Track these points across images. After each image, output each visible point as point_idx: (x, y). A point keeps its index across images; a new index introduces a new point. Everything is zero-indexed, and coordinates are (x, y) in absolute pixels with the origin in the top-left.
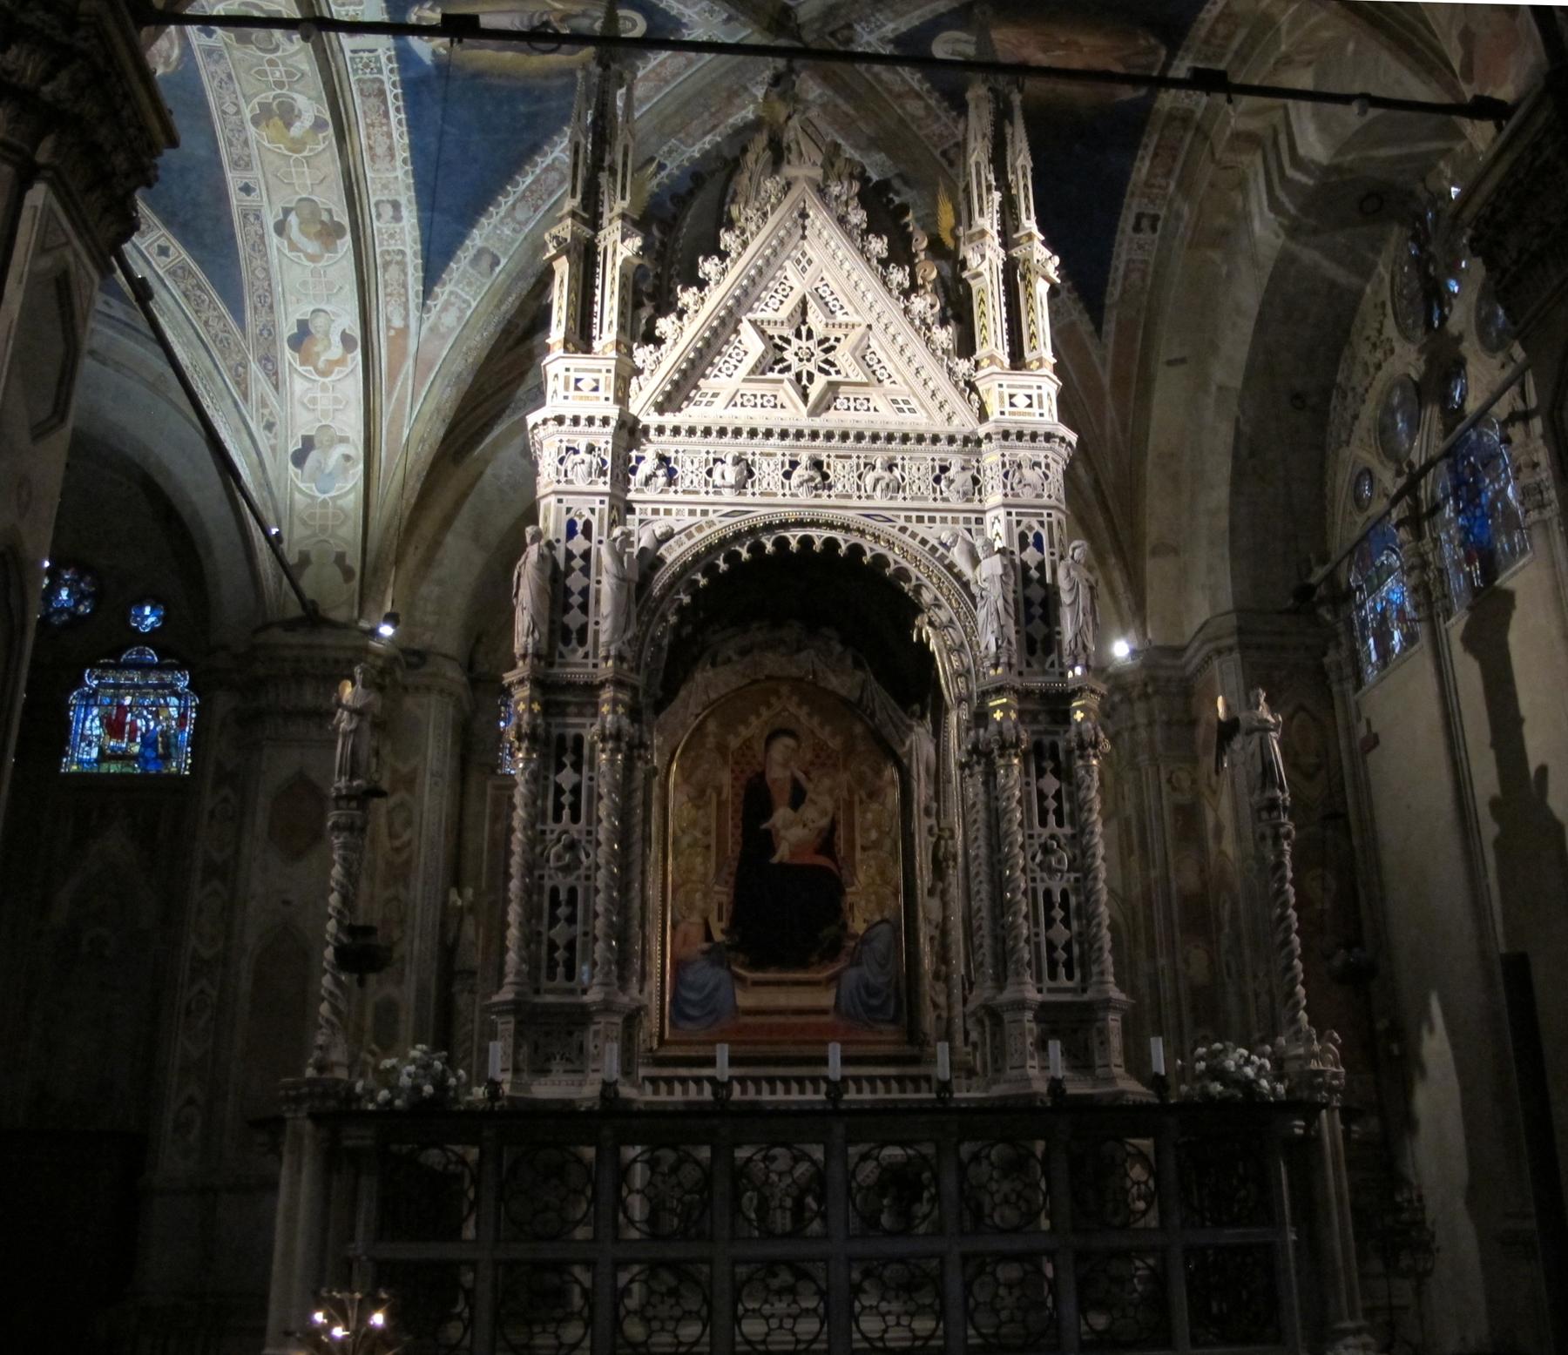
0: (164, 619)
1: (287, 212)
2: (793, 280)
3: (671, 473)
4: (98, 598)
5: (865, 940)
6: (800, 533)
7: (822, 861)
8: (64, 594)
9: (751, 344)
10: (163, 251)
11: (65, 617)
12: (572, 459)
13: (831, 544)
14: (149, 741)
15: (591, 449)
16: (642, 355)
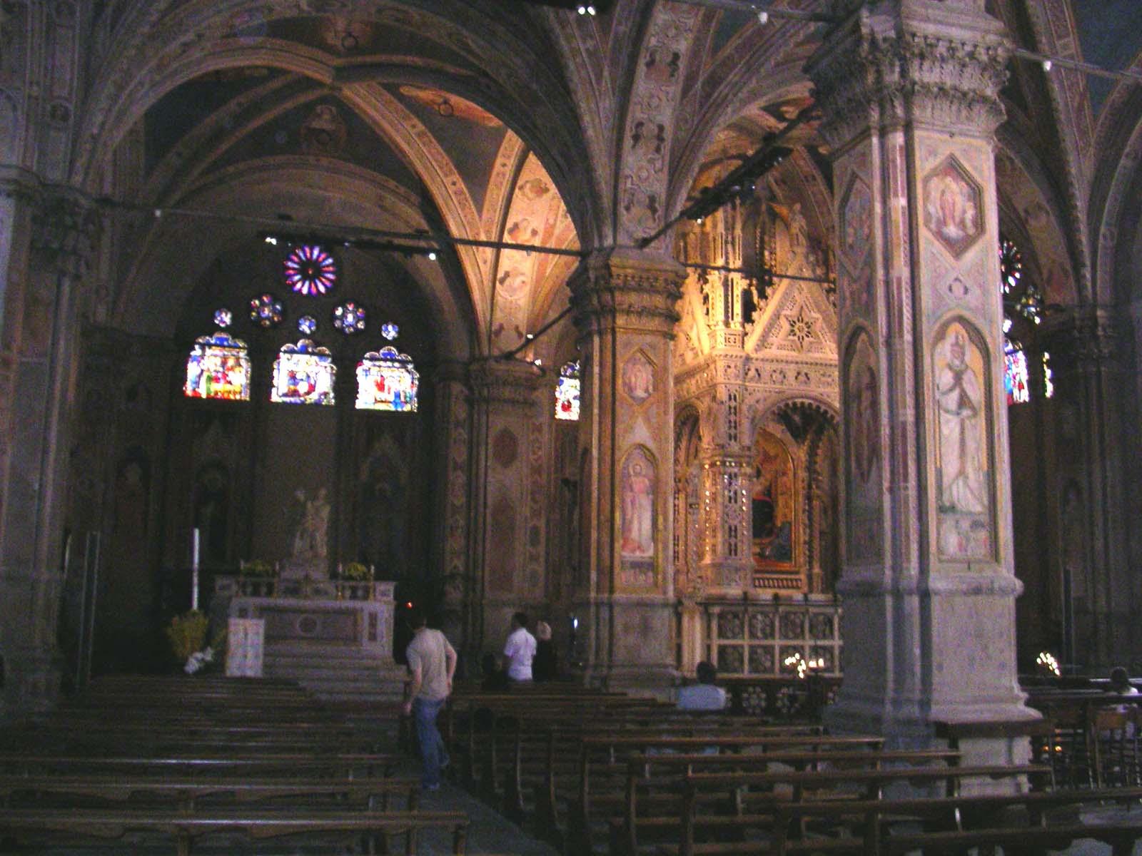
0: (399, 333)
1: (527, 182)
2: (797, 298)
3: (759, 375)
4: (366, 319)
5: (781, 529)
6: (800, 400)
7: (767, 499)
8: (350, 318)
9: (786, 326)
10: (454, 184)
11: (352, 330)
12: (729, 370)
13: (810, 404)
14: (398, 395)
15: (736, 367)
16: (748, 327)
